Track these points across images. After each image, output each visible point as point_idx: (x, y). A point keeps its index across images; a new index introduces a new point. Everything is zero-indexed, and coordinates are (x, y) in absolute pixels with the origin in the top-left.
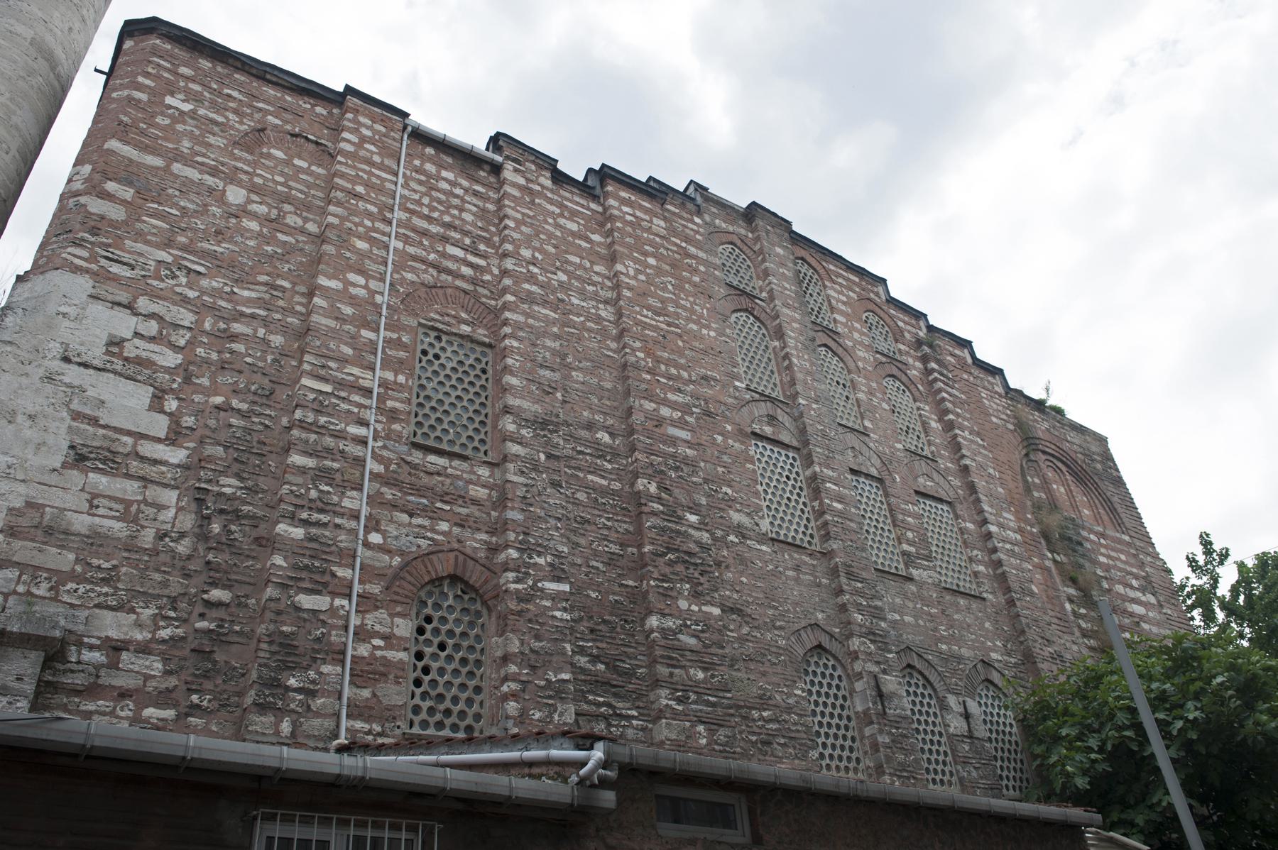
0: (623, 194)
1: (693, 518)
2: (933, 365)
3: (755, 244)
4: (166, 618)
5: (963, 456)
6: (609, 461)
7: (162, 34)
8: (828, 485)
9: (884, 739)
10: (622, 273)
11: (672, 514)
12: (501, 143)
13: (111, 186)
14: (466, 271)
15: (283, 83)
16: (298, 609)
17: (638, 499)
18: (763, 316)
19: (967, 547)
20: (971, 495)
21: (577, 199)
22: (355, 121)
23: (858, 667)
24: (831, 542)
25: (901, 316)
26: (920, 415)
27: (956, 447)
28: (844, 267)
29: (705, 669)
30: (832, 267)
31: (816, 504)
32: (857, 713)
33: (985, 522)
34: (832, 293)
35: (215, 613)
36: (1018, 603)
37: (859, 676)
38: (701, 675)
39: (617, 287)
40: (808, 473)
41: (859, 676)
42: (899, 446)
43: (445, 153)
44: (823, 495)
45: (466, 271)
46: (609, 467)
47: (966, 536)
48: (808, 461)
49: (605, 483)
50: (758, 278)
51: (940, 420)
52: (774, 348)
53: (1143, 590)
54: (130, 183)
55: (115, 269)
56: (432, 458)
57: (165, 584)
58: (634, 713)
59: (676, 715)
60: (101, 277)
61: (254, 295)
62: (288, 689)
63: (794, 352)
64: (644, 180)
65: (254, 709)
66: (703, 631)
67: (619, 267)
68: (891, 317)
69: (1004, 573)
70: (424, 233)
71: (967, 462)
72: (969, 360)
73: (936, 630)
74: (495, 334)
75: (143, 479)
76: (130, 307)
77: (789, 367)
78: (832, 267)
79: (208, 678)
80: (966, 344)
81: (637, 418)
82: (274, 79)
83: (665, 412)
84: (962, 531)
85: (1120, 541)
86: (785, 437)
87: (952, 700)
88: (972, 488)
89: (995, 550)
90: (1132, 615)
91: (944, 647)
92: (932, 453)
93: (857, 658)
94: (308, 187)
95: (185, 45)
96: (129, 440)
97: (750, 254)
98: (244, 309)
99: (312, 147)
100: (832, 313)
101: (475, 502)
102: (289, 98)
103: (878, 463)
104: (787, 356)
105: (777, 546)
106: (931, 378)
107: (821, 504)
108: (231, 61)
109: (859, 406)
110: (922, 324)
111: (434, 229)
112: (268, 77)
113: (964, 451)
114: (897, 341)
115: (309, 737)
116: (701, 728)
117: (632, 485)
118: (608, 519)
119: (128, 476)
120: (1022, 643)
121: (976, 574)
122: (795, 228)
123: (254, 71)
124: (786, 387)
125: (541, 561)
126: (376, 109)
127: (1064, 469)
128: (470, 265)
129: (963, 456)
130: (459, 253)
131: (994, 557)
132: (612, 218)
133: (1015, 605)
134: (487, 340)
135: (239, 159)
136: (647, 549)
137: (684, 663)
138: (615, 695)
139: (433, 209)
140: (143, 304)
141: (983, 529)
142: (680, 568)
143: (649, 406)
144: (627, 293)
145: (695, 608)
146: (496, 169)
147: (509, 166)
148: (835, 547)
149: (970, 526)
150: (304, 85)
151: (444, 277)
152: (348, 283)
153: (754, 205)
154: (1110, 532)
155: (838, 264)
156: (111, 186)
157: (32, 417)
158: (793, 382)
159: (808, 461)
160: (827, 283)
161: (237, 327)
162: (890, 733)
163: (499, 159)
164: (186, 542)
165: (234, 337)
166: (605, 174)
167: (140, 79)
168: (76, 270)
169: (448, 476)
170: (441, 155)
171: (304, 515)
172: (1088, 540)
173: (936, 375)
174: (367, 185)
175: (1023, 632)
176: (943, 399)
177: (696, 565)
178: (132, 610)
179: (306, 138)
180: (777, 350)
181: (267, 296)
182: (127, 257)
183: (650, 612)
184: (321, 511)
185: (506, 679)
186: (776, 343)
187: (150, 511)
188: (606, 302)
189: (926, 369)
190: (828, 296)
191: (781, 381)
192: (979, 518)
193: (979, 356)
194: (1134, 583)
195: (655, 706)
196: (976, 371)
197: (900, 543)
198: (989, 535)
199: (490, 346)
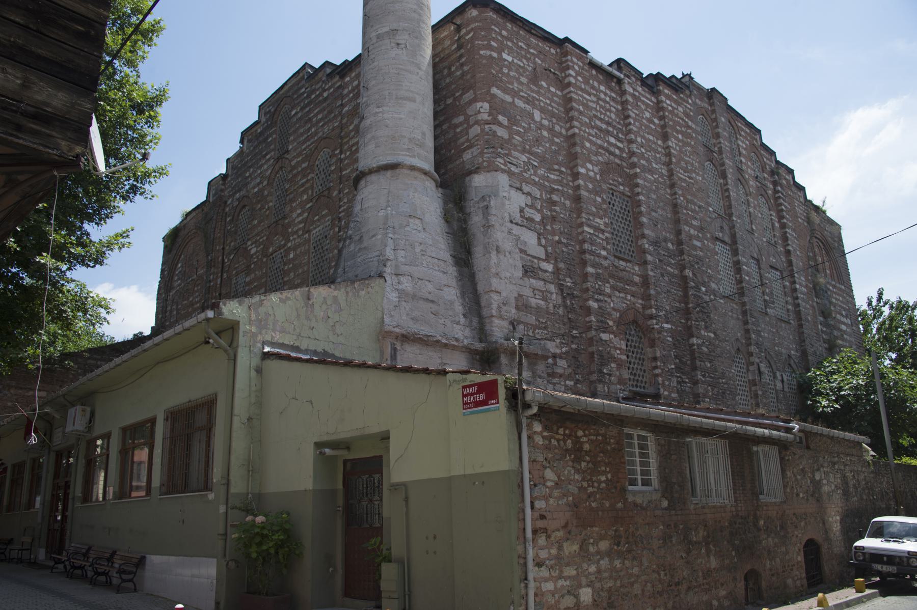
0: (666, 91)
1: (703, 289)
2: (779, 188)
3: (712, 114)
4: (563, 343)
5: (788, 245)
6: (673, 259)
7: (492, 8)
8: (744, 267)
9: (760, 393)
10: (673, 147)
11: (697, 288)
12: (622, 65)
13: (500, 118)
14: (617, 152)
15: (537, 34)
16: (601, 340)
17: (685, 279)
18: (717, 164)
19: (786, 296)
20: (789, 266)
21: (647, 95)
22: (572, 61)
23: (752, 359)
24: (745, 298)
25: (767, 156)
26: (771, 219)
27: (785, 239)
28: (744, 124)
29: (710, 362)
30: (739, 125)
31: (738, 276)
32: (749, 380)
33: (794, 282)
34: (740, 143)
35: (576, 341)
36: (804, 326)
37: (753, 364)
38: (709, 365)
39: (669, 155)
40: (735, 259)
41: (753, 364)
42: (765, 240)
43: (601, 74)
44: (742, 273)
45: (617, 152)
46: (673, 262)
47: (786, 290)
48: (735, 252)
49: (672, 271)
50: (714, 138)
51: (779, 222)
52: (721, 184)
53: (846, 317)
54: (504, 115)
55: (513, 168)
56: (621, 262)
57: (559, 329)
58: (687, 380)
59: (703, 382)
60: (510, 174)
61: (556, 178)
62: (604, 373)
63: (730, 188)
64: (668, 76)
65: (597, 382)
66: (709, 345)
67: (670, 144)
68: (761, 155)
69: (800, 310)
70: (600, 129)
71: (790, 248)
72: (792, 183)
73: (774, 340)
74: (632, 190)
75: (544, 280)
76: (520, 189)
77: (729, 197)
78: (739, 125)
79: (578, 368)
80: (791, 172)
81: (683, 236)
82: (535, 32)
83: (692, 231)
84: (784, 287)
85: (841, 289)
86: (727, 239)
87: (778, 374)
88: (790, 263)
89: (797, 298)
90: (841, 330)
91: (777, 348)
92: (775, 242)
93: (752, 355)
94: (557, 105)
95: (500, 14)
96: (536, 261)
97: (709, 119)
98: (554, 186)
99: (551, 75)
100: (740, 156)
101: (636, 284)
102: (540, 44)
103: (756, 249)
104: (727, 190)
105: (726, 299)
106: (777, 195)
107: (741, 277)
108: (518, 23)
109: (750, 216)
110: (773, 158)
111: (604, 126)
112: (533, 31)
113: (789, 242)
114: (763, 171)
115: (613, 392)
116: (709, 388)
117: (681, 271)
118: (675, 290)
119: (539, 279)
120: (802, 346)
121: (788, 310)
122: (729, 103)
123: (527, 28)
124: (726, 209)
125: (661, 314)
126: (577, 50)
127: (822, 247)
128: (619, 148)
129: (788, 245)
130: (612, 140)
131: (796, 301)
132: (663, 109)
133: (802, 327)
134: (629, 194)
135: (533, 91)
136: (691, 305)
137: (704, 360)
138: (682, 373)
139: (601, 113)
140: (526, 188)
141: (793, 286)
142: (701, 315)
143: (687, 228)
144: (674, 160)
145: (706, 334)
146: (619, 82)
147: (626, 80)
148: (746, 300)
149: (787, 284)
150: (546, 35)
151: (612, 157)
152: (588, 170)
153: (714, 90)
154: (838, 285)
155: (742, 122)
156: (500, 118)
157: (510, 253)
158: (730, 207)
159: (735, 252)
160: (738, 137)
161: (555, 198)
162: (762, 390)
163: (622, 76)
164: (561, 309)
165: (554, 203)
166: (658, 77)
167: (493, 43)
168: (503, 171)
169: (627, 271)
170: (599, 75)
171: (596, 297)
172: (829, 289)
173: (780, 194)
174: (583, 104)
175: (804, 341)
176: (782, 210)
177: (705, 313)
178: (554, 341)
179: (550, 70)
180: (722, 185)
181: (560, 178)
182: (515, 162)
183: (693, 336)
184: (600, 294)
185: (656, 367)
186: (722, 181)
187: (549, 295)
188: (664, 164)
189: (775, 189)
190: (738, 145)
191: (724, 204)
192: (792, 280)
193: (797, 180)
194: (844, 313)
195: (696, 378)
196: (794, 189)
197: (764, 295)
198: (795, 290)
199: (629, 197)
